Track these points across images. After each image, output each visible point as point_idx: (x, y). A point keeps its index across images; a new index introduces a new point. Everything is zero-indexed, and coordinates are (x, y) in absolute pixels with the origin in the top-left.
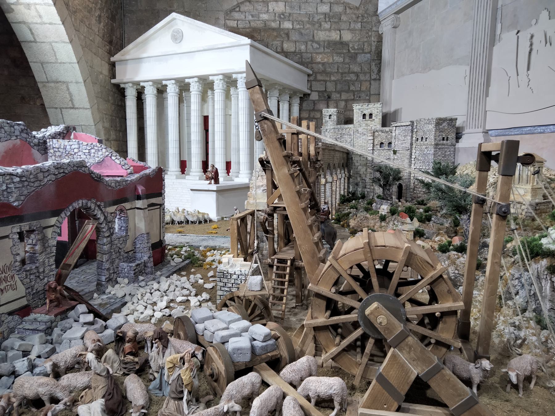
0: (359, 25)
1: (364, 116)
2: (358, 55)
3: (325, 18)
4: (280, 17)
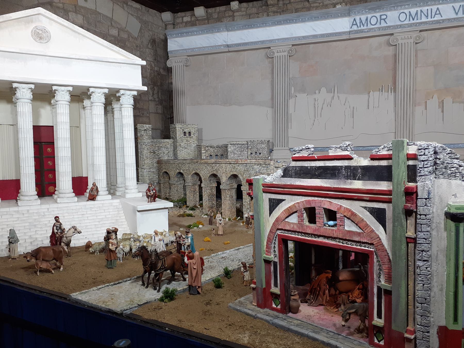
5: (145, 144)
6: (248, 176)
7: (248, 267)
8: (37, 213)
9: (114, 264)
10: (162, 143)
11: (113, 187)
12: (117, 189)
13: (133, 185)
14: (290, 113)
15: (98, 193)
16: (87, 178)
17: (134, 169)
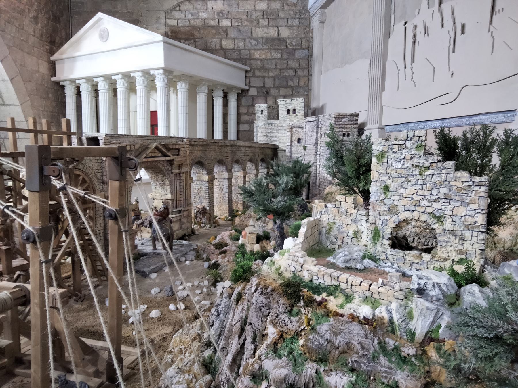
0: (296, 22)
1: (288, 111)
2: (296, 51)
3: (263, 16)
4: (219, 15)
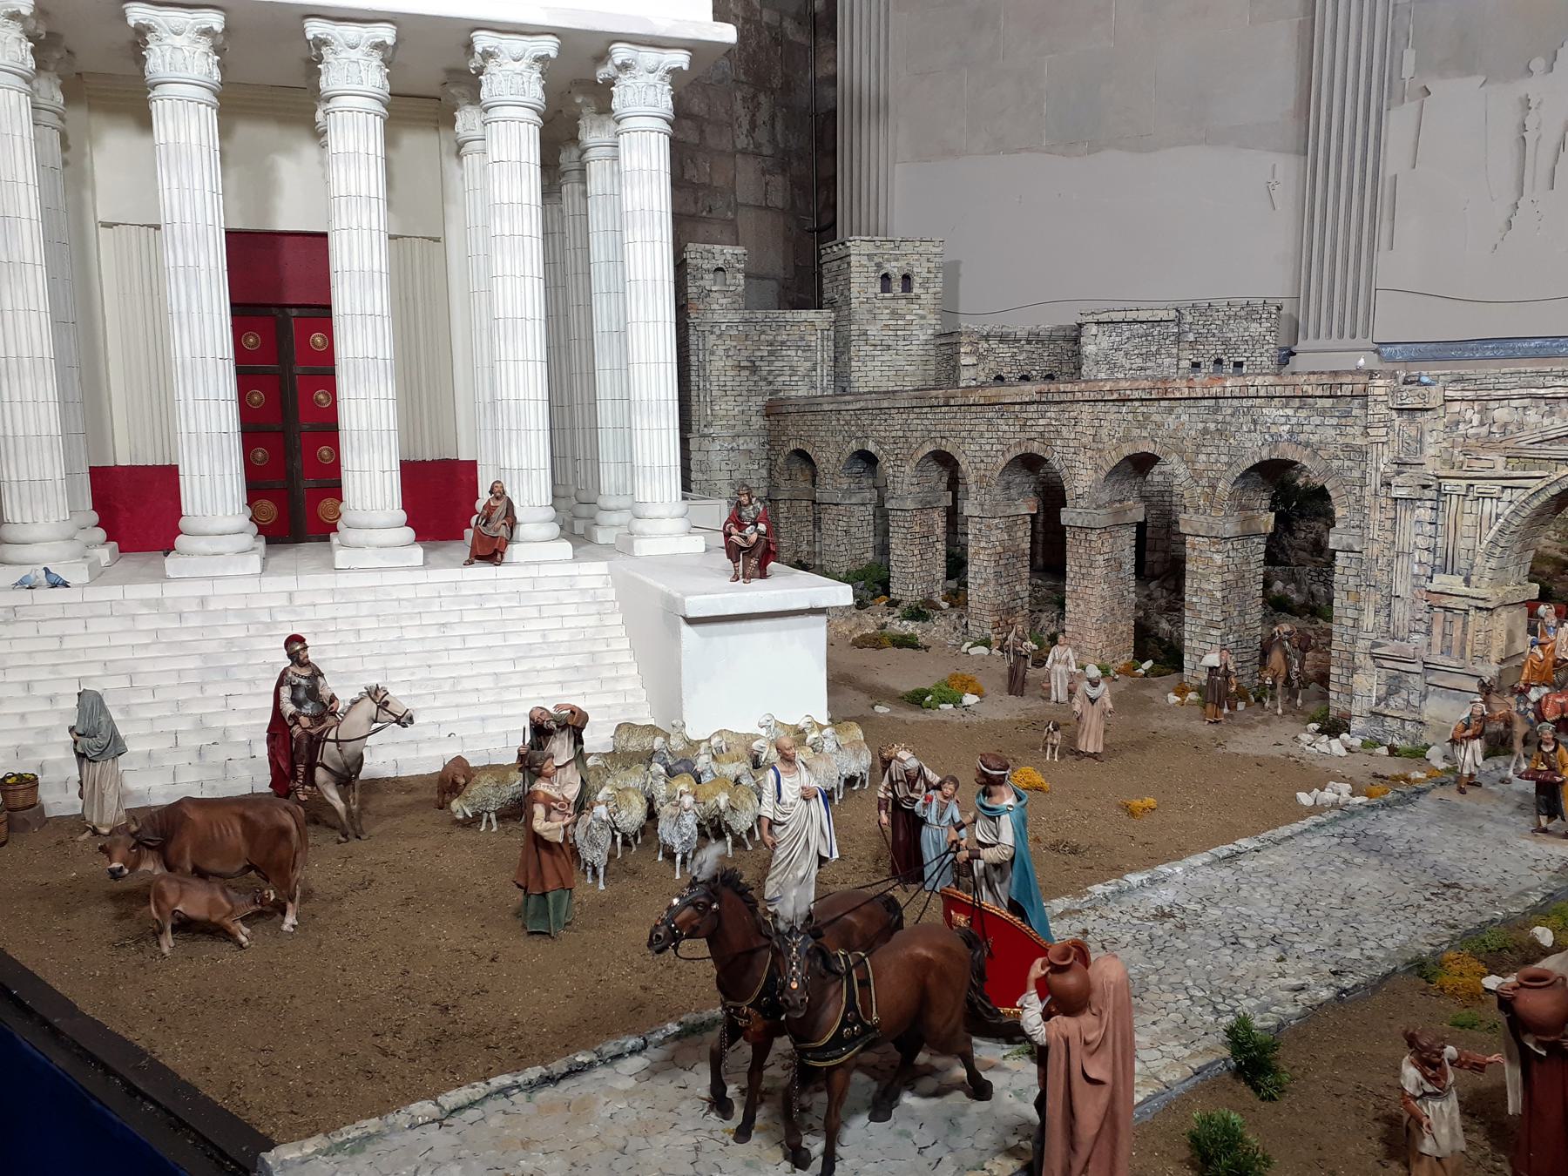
1: (886, 278)
5: (718, 332)
6: (1224, 459)
7: (1452, 1063)
8: (239, 612)
9: (557, 911)
10: (788, 328)
11: (583, 510)
12: (602, 517)
13: (667, 500)
14: (1389, 173)
15: (512, 529)
16: (472, 466)
17: (671, 426)
